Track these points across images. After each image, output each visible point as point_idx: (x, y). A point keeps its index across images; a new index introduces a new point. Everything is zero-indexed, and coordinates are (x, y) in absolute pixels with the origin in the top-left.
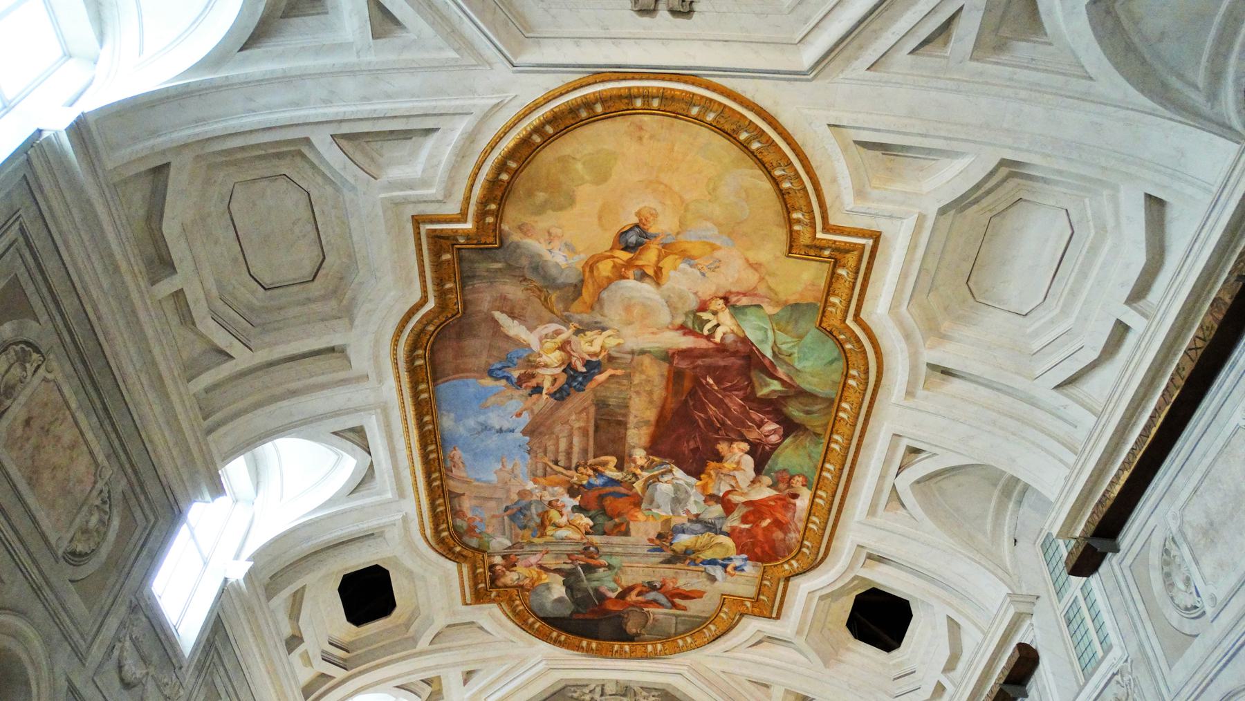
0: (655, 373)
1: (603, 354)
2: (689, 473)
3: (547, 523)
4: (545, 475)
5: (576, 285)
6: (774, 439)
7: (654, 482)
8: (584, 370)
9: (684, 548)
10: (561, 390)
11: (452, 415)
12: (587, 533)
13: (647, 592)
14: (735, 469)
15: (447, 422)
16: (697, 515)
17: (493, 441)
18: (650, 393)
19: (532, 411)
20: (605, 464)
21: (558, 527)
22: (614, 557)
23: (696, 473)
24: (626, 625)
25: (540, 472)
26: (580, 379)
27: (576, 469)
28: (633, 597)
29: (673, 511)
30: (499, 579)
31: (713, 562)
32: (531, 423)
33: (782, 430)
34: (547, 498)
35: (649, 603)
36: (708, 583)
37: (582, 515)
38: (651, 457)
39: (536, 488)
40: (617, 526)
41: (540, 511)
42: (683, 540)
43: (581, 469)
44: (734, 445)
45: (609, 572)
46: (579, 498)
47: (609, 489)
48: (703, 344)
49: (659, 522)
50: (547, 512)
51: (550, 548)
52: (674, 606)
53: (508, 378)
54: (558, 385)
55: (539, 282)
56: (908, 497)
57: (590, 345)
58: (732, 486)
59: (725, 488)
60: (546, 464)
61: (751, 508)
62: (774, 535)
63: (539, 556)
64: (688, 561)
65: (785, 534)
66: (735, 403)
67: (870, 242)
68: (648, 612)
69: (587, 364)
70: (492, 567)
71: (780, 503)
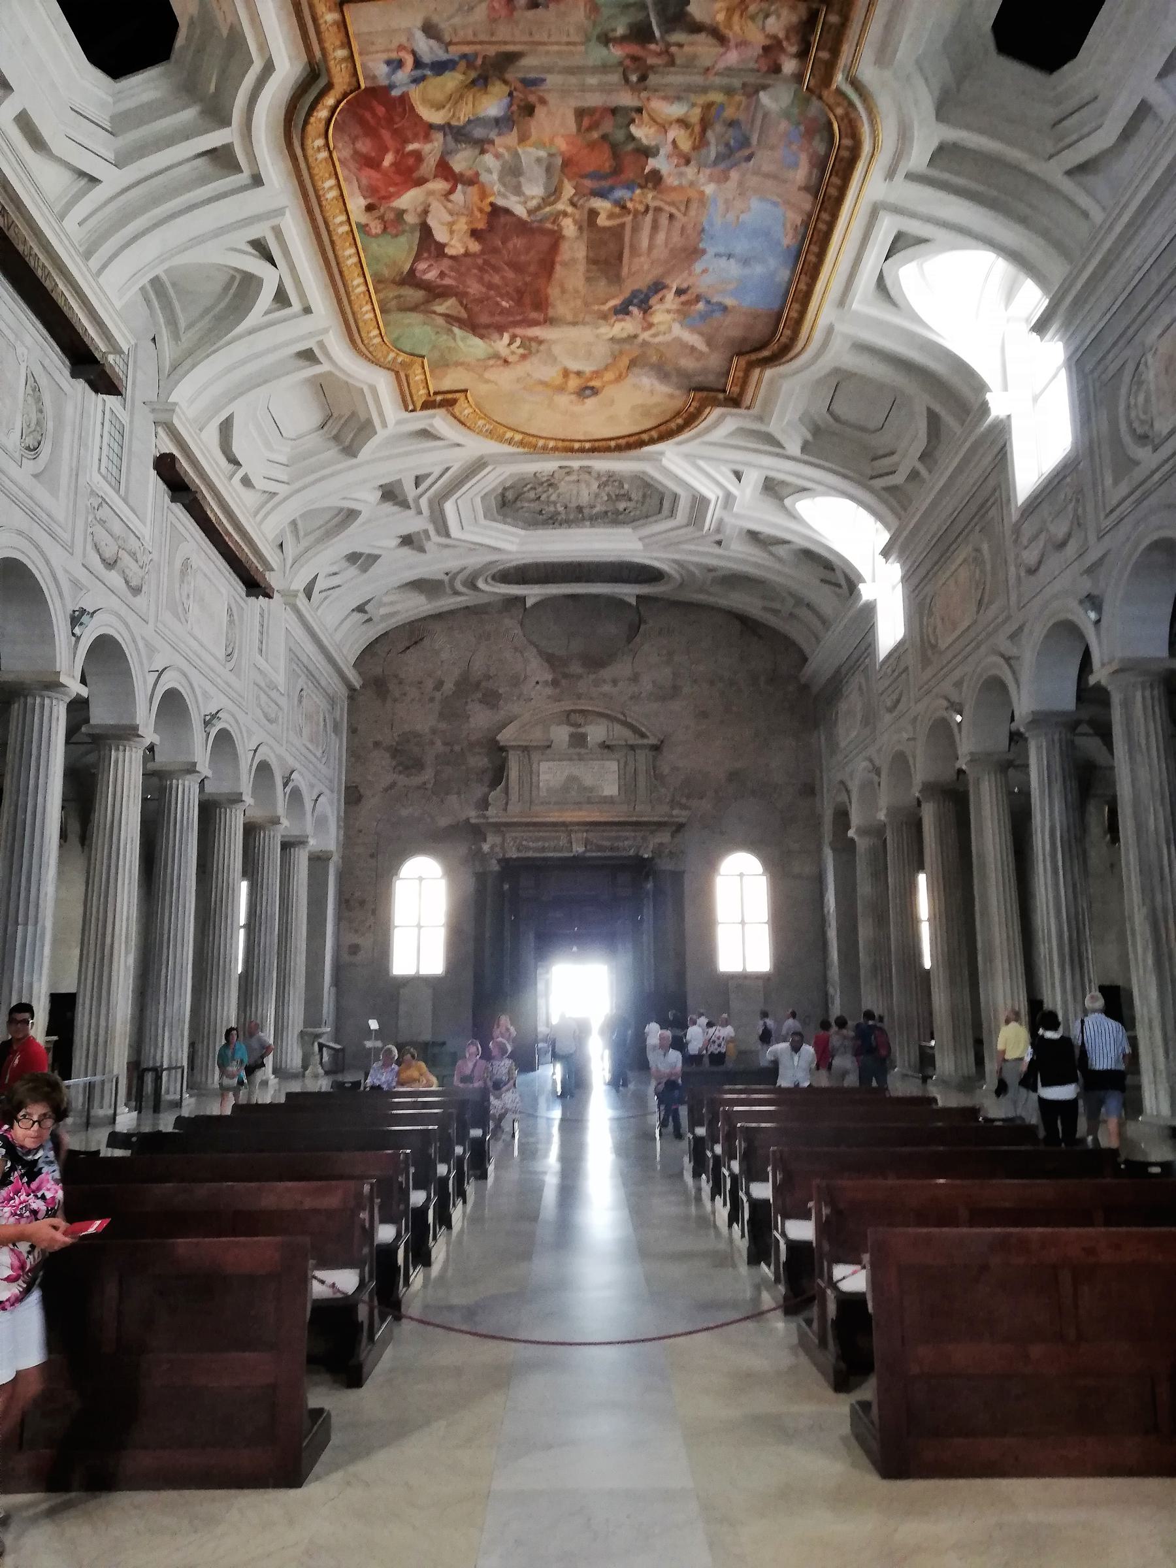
0: (560, 308)
1: (613, 321)
2: (507, 211)
3: (697, 129)
4: (688, 202)
5: (635, 365)
6: (422, 266)
7: (549, 197)
8: (631, 308)
9: (490, 88)
10: (656, 292)
11: (777, 279)
12: (639, 110)
15: (784, 274)
16: (483, 152)
17: (741, 247)
18: (563, 291)
20: (611, 216)
21: (683, 122)
22: (599, 63)
23: (497, 212)
25: (694, 206)
26: (635, 301)
29: (516, 155)
31: (440, 67)
32: (696, 260)
33: (418, 274)
34: (690, 171)
36: (435, 19)
37: (645, 141)
38: (556, 228)
39: (703, 185)
41: (704, 151)
42: (492, 105)
43: (641, 208)
44: (462, 251)
46: (646, 171)
47: (605, 184)
48: (519, 331)
49: (533, 138)
51: (698, 80)
53: (708, 302)
54: (660, 295)
55: (668, 368)
56: (255, 265)
57: (624, 327)
58: (449, 201)
59: (458, 196)
60: (685, 214)
61: (415, 175)
63: (721, 65)
64: (479, 61)
66: (474, 288)
67: (411, 407)
69: (628, 313)
70: (803, 55)
71: (383, 193)
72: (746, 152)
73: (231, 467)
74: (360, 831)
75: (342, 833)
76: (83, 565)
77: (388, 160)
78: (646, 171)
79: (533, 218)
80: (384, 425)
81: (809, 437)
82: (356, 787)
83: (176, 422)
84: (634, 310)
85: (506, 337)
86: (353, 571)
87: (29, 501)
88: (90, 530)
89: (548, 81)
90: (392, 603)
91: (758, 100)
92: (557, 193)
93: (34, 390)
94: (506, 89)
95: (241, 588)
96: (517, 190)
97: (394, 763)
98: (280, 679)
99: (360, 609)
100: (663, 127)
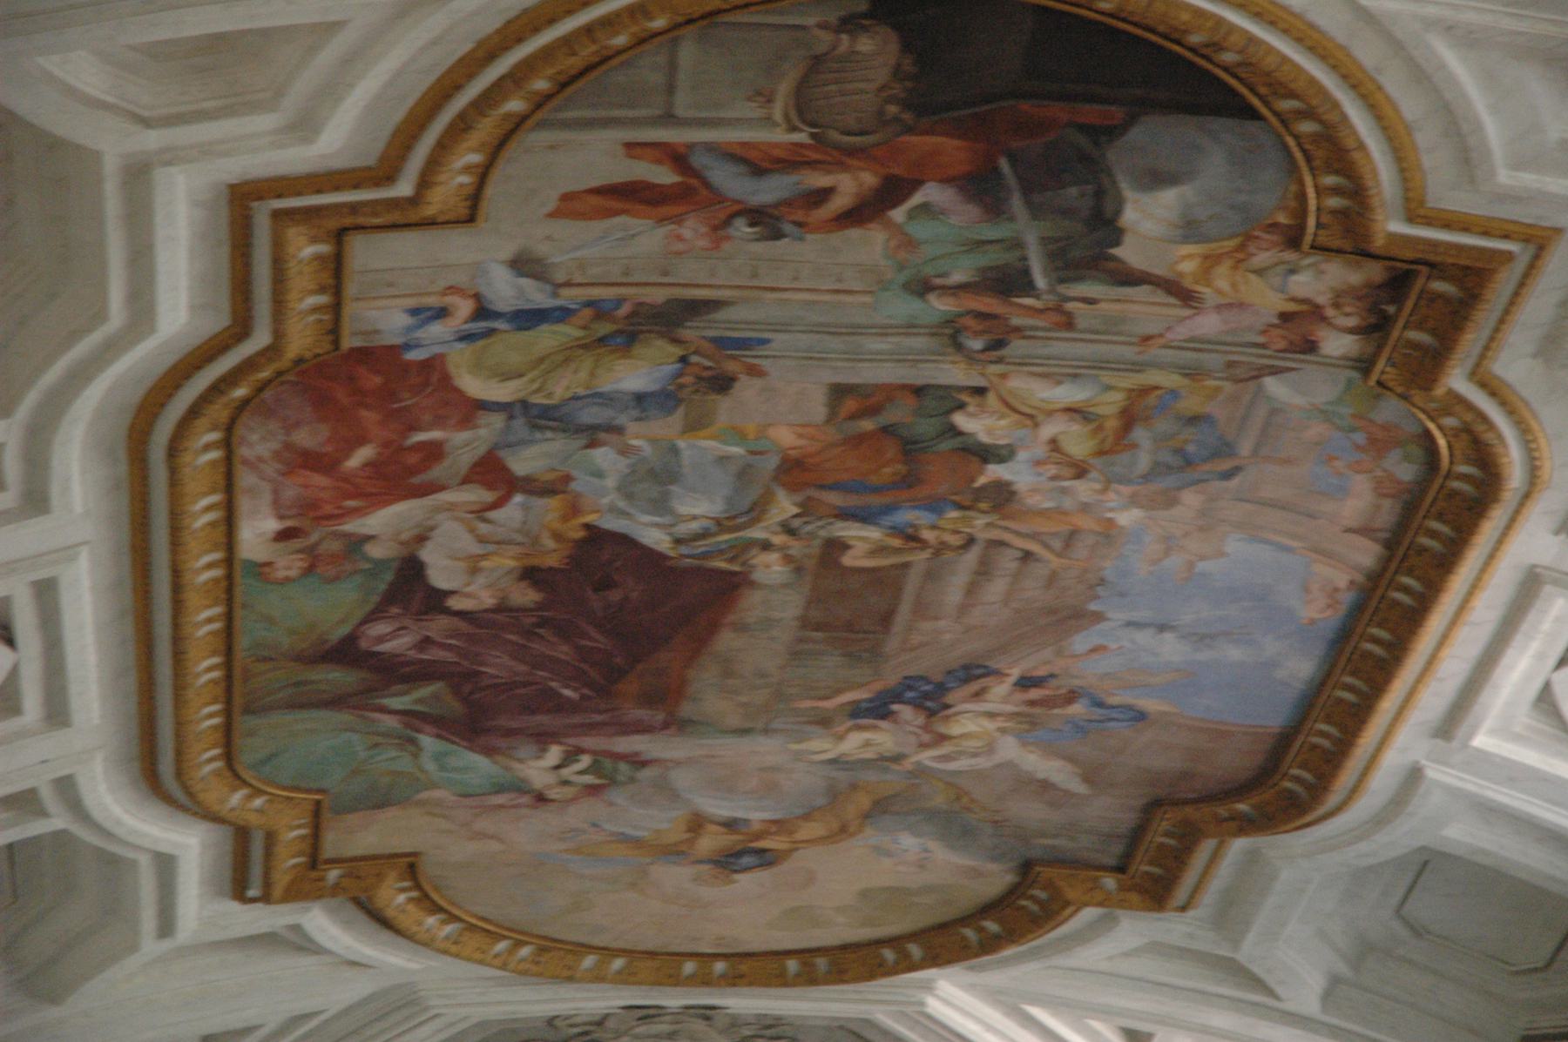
3: (1112, 424)
9: (638, 350)
10: (967, 680)
12: (980, 391)
13: (787, 203)
14: (484, 557)
15: (1300, 668)
16: (592, 444)
18: (728, 673)
19: (1059, 653)
20: (880, 550)
23: (596, 537)
24: (897, 73)
27: (971, 541)
28: (849, 186)
29: (675, 451)
30: (1368, 285)
31: (528, 318)
33: (364, 644)
34: (1084, 490)
35: (790, 161)
36: (542, 249)
37: (985, 439)
38: (736, 568)
39: (1111, 510)
40: (873, 411)
41: (1124, 458)
44: (488, 601)
45: (929, 270)
47: (875, 500)
50: (1101, 453)
52: (678, 158)
53: (1100, 704)
54: (975, 686)
61: (416, 480)
62: (324, 431)
63: (1182, 332)
64: (624, 310)
65: (288, 446)
68: (793, 129)
71: (328, 509)
72: (1226, 465)
77: (360, 457)
78: (977, 484)
79: (684, 550)
80: (166, 926)
81: (1343, 969)
84: (905, 711)
85: (554, 754)
89: (773, 345)
91: (1260, 389)
92: (753, 514)
94: (678, 351)
96: (660, 505)
100: (1031, 419)
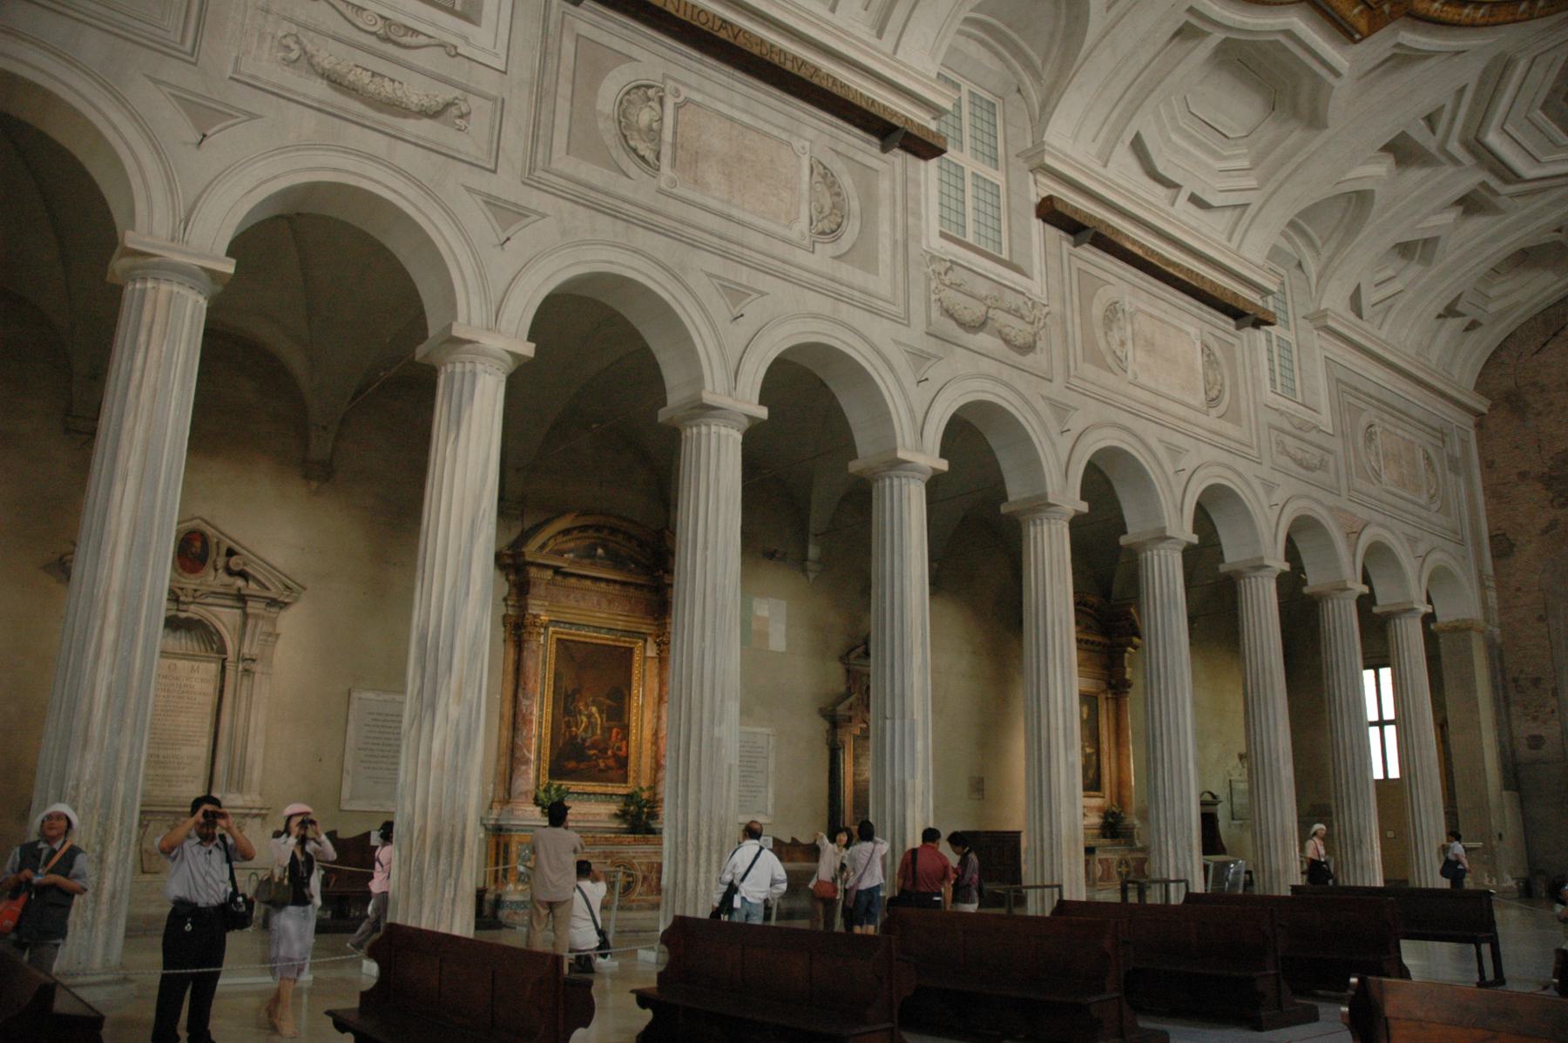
67: (1357, 37)
73: (1170, 192)
74: (1518, 590)
75: (1492, 595)
76: (928, 333)
82: (1504, 534)
83: (1049, 161)
86: (1414, 269)
87: (830, 283)
88: (933, 297)
90: (1505, 295)
93: (824, 177)
95: (1228, 323)
97: (1551, 495)
98: (1325, 419)
99: (1450, 312)
